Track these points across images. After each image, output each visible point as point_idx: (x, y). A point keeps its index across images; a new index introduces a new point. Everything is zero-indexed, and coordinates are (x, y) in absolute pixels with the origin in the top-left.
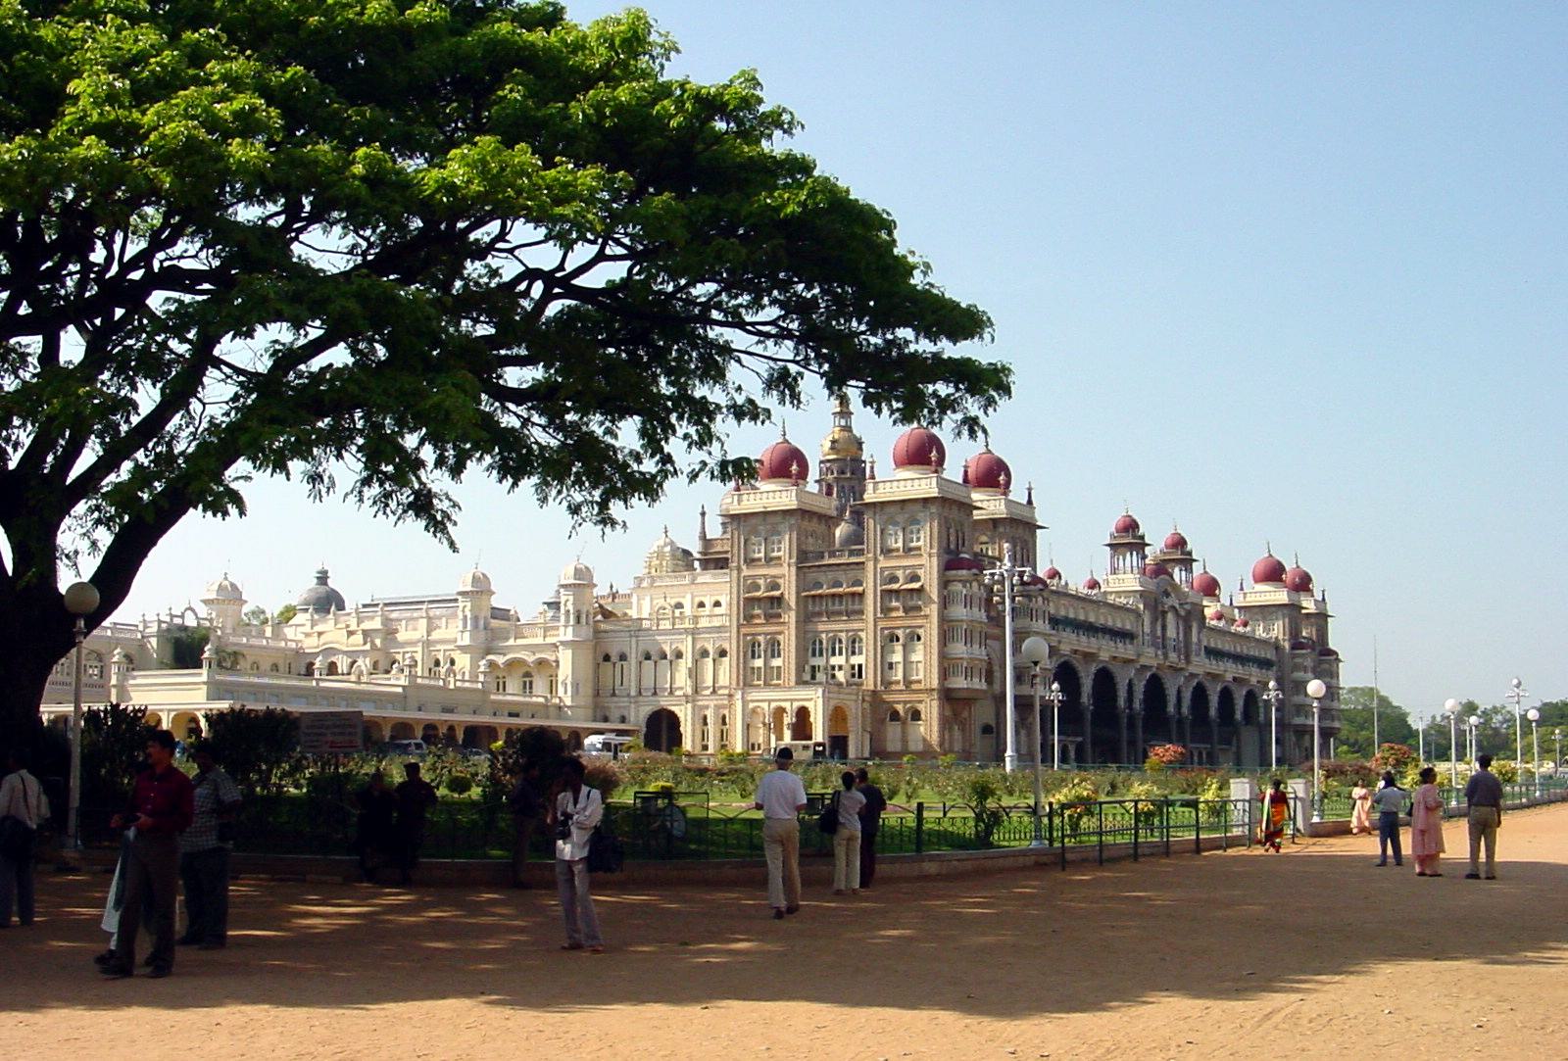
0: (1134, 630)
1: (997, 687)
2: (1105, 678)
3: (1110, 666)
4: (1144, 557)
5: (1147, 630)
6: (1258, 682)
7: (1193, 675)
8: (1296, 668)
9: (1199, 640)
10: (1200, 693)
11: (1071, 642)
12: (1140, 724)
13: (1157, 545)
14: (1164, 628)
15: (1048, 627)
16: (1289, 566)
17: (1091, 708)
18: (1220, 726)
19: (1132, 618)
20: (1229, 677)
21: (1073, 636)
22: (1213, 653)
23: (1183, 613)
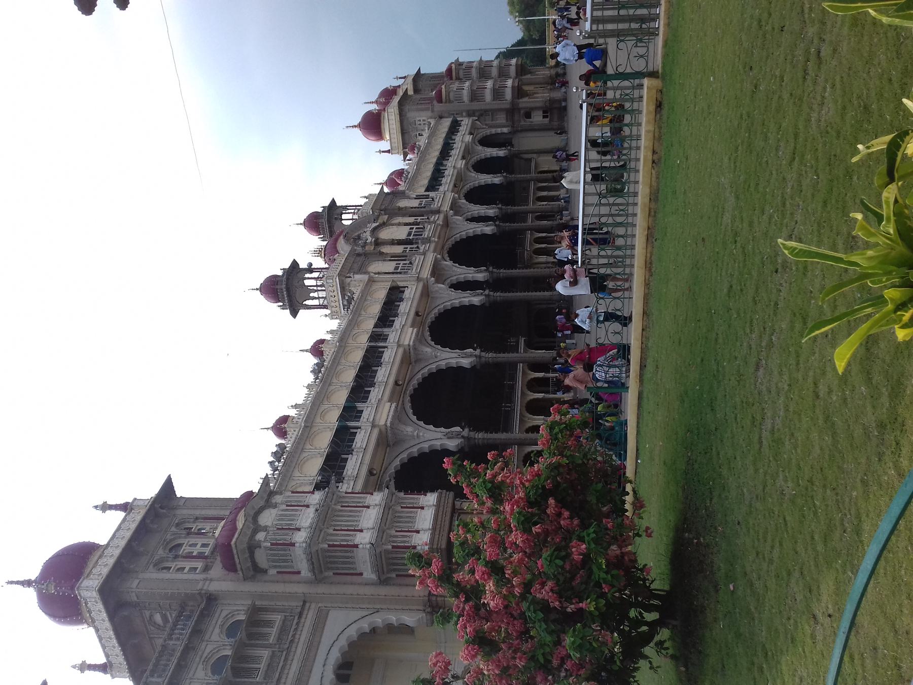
0: (388, 285)
1: (409, 619)
2: (446, 328)
3: (429, 320)
4: (310, 269)
5: (390, 266)
6: (471, 133)
7: (454, 206)
8: (459, 99)
9: (418, 197)
10: (477, 195)
11: (379, 410)
12: (503, 272)
13: (306, 248)
14: (393, 242)
15: (318, 497)
16: (374, 107)
17: (478, 351)
18: (511, 173)
19: (375, 286)
20: (461, 164)
21: (375, 394)
22: (434, 183)
23: (386, 217)
